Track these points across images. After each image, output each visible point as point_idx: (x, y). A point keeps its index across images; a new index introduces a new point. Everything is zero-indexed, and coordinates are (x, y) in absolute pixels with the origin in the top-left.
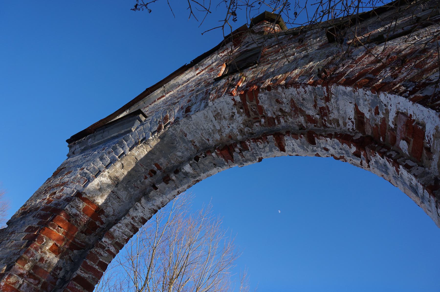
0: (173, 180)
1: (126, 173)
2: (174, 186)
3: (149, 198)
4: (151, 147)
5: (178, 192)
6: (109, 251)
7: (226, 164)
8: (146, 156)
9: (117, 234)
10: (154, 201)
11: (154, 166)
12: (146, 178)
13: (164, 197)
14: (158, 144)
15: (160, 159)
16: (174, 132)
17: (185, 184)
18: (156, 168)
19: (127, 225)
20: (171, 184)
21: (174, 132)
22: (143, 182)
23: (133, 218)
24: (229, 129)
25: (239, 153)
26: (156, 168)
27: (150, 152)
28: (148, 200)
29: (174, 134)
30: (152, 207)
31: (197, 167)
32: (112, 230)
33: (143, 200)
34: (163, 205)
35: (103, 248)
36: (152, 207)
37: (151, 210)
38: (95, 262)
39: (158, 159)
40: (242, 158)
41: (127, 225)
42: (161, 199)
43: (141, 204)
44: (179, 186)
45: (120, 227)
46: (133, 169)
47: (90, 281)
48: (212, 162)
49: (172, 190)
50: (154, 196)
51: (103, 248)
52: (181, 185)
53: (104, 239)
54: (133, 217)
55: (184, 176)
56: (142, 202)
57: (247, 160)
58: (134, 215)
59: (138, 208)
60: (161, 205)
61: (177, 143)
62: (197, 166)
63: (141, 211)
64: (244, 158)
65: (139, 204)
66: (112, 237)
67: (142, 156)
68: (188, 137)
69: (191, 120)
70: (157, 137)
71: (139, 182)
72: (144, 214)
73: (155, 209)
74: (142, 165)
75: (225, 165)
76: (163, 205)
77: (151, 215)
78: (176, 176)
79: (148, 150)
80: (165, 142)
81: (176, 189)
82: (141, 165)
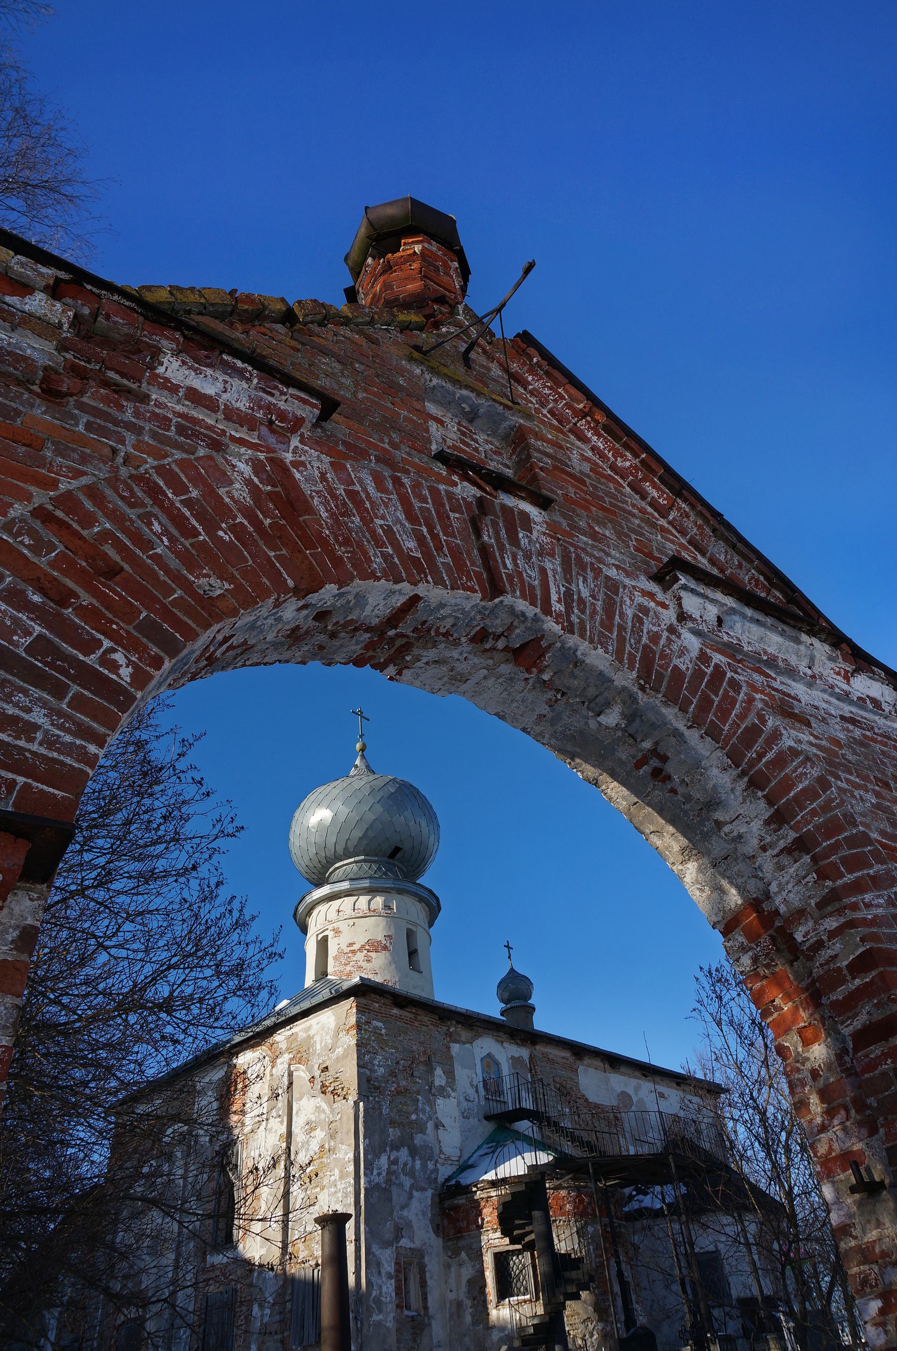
0: (656, 743)
1: (671, 829)
2: (673, 741)
3: (710, 801)
4: (600, 775)
5: (689, 728)
7: (558, 645)
8: (623, 783)
10: (720, 790)
11: (641, 772)
13: (708, 764)
14: (586, 761)
15: (620, 759)
16: (547, 736)
17: (663, 715)
20: (669, 747)
21: (547, 736)
22: (684, 797)
24: (470, 656)
25: (506, 637)
27: (614, 776)
28: (718, 804)
29: (551, 735)
30: (738, 793)
31: (600, 700)
33: (719, 815)
34: (731, 767)
36: (738, 793)
37: (748, 796)
39: (621, 763)
40: (516, 627)
42: (715, 771)
43: (727, 823)
44: (669, 729)
46: (661, 812)
48: (572, 673)
49: (686, 742)
50: (706, 790)
52: (666, 724)
54: (761, 847)
55: (638, 721)
56: (722, 819)
57: (517, 616)
59: (735, 834)
60: (731, 771)
61: (570, 730)
62: (597, 700)
63: (745, 825)
64: (515, 624)
65: (726, 829)
67: (625, 792)
68: (544, 712)
69: (503, 711)
70: (573, 763)
71: (687, 807)
72: (756, 817)
73: (744, 787)
74: (647, 795)
75: (563, 647)
76: (731, 767)
77: (759, 798)
78: (642, 741)
79: (609, 779)
80: (578, 750)
81: (683, 734)
82: (646, 796)
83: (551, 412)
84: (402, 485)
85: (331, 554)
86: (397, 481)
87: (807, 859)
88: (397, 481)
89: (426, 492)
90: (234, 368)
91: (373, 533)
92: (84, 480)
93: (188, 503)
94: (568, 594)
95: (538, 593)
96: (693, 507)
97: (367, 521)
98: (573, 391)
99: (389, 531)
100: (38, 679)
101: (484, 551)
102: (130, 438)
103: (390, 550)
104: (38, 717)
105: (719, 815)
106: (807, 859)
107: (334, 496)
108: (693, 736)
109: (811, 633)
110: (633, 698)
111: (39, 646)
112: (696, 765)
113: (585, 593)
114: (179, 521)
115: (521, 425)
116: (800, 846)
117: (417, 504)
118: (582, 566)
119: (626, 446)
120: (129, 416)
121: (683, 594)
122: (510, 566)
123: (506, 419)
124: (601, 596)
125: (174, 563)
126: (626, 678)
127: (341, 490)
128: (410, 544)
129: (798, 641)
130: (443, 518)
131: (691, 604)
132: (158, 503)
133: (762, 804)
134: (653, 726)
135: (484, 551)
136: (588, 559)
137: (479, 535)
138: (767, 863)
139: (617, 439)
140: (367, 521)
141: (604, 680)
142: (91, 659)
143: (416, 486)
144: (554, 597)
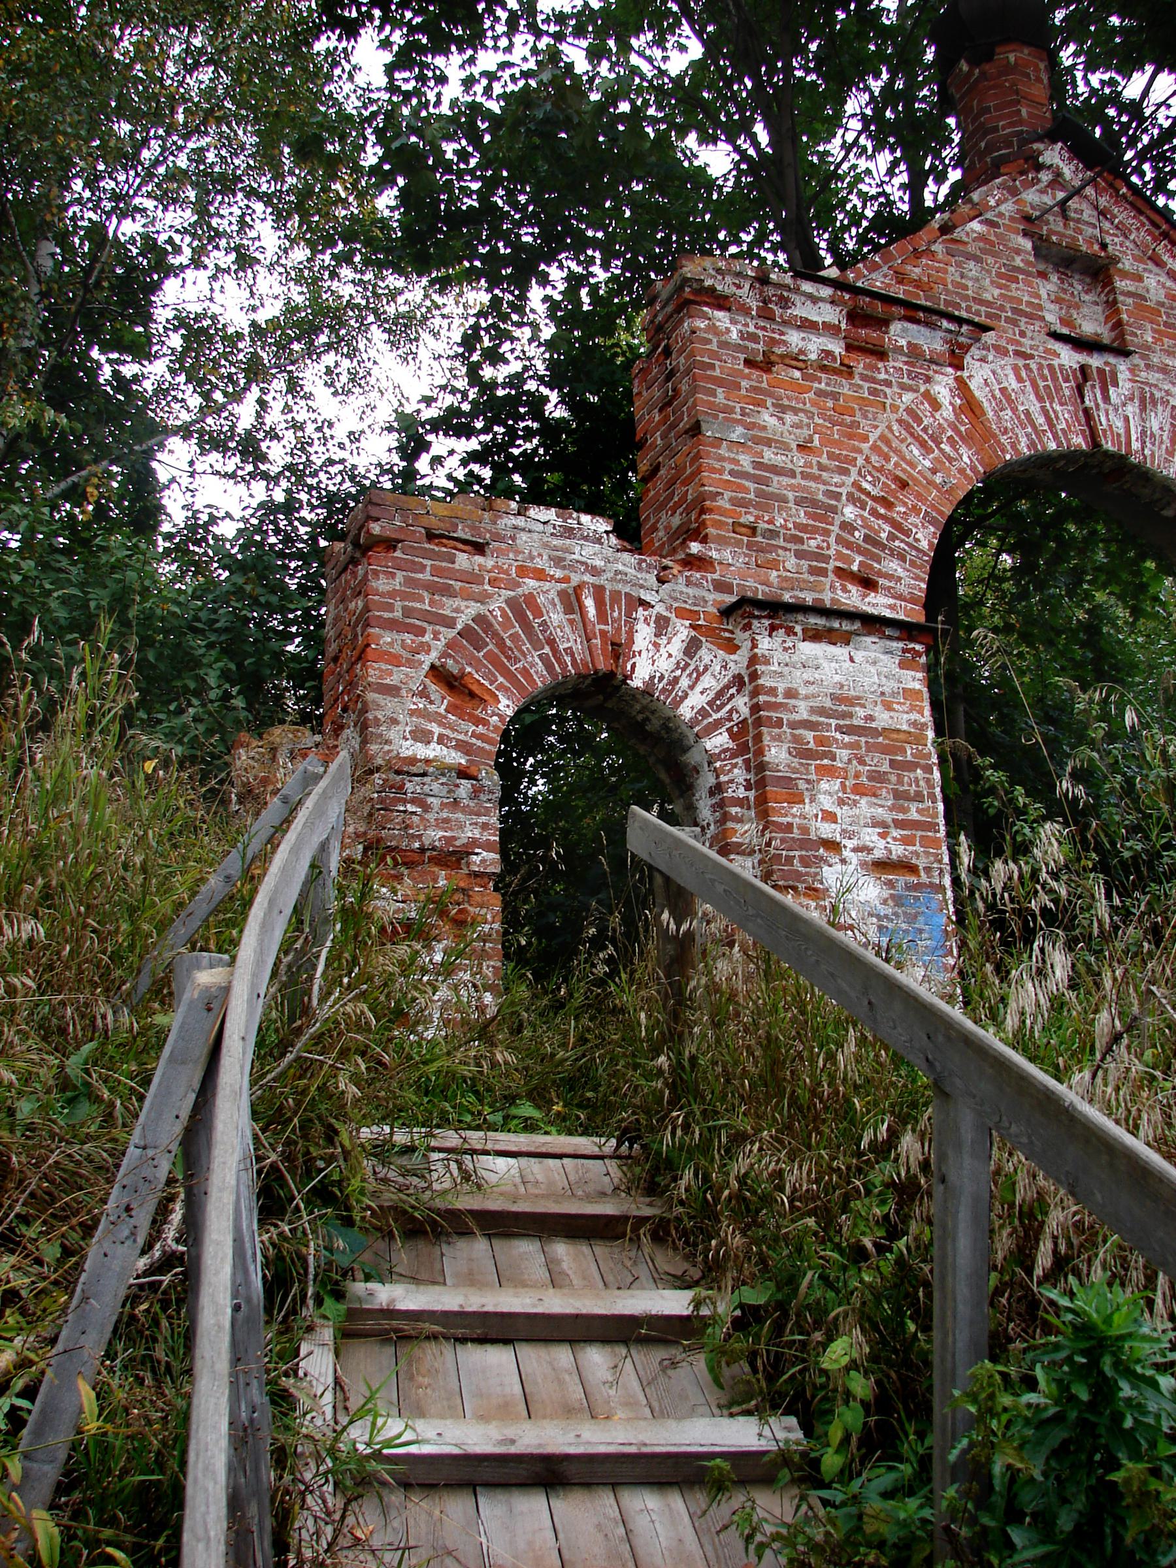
84: (1031, 371)
85: (998, 442)
86: (1027, 367)
88: (1027, 367)
89: (1046, 372)
91: (1018, 418)
92: (878, 432)
93: (925, 430)
94: (1143, 433)
95: (1123, 439)
97: (1014, 410)
99: (1027, 413)
100: (894, 553)
101: (1086, 411)
102: (888, 391)
103: (1029, 430)
104: (900, 572)
107: (994, 396)
111: (892, 537)
113: (1155, 428)
114: (923, 444)
117: (1041, 384)
118: (1154, 402)
120: (883, 376)
122: (1103, 419)
124: (1166, 428)
125: (929, 474)
127: (996, 387)
128: (1041, 420)
130: (1058, 389)
132: (912, 435)
135: (1086, 411)
136: (1158, 395)
137: (1083, 402)
140: (1014, 410)
142: (911, 540)
143: (1040, 367)
144: (1133, 438)
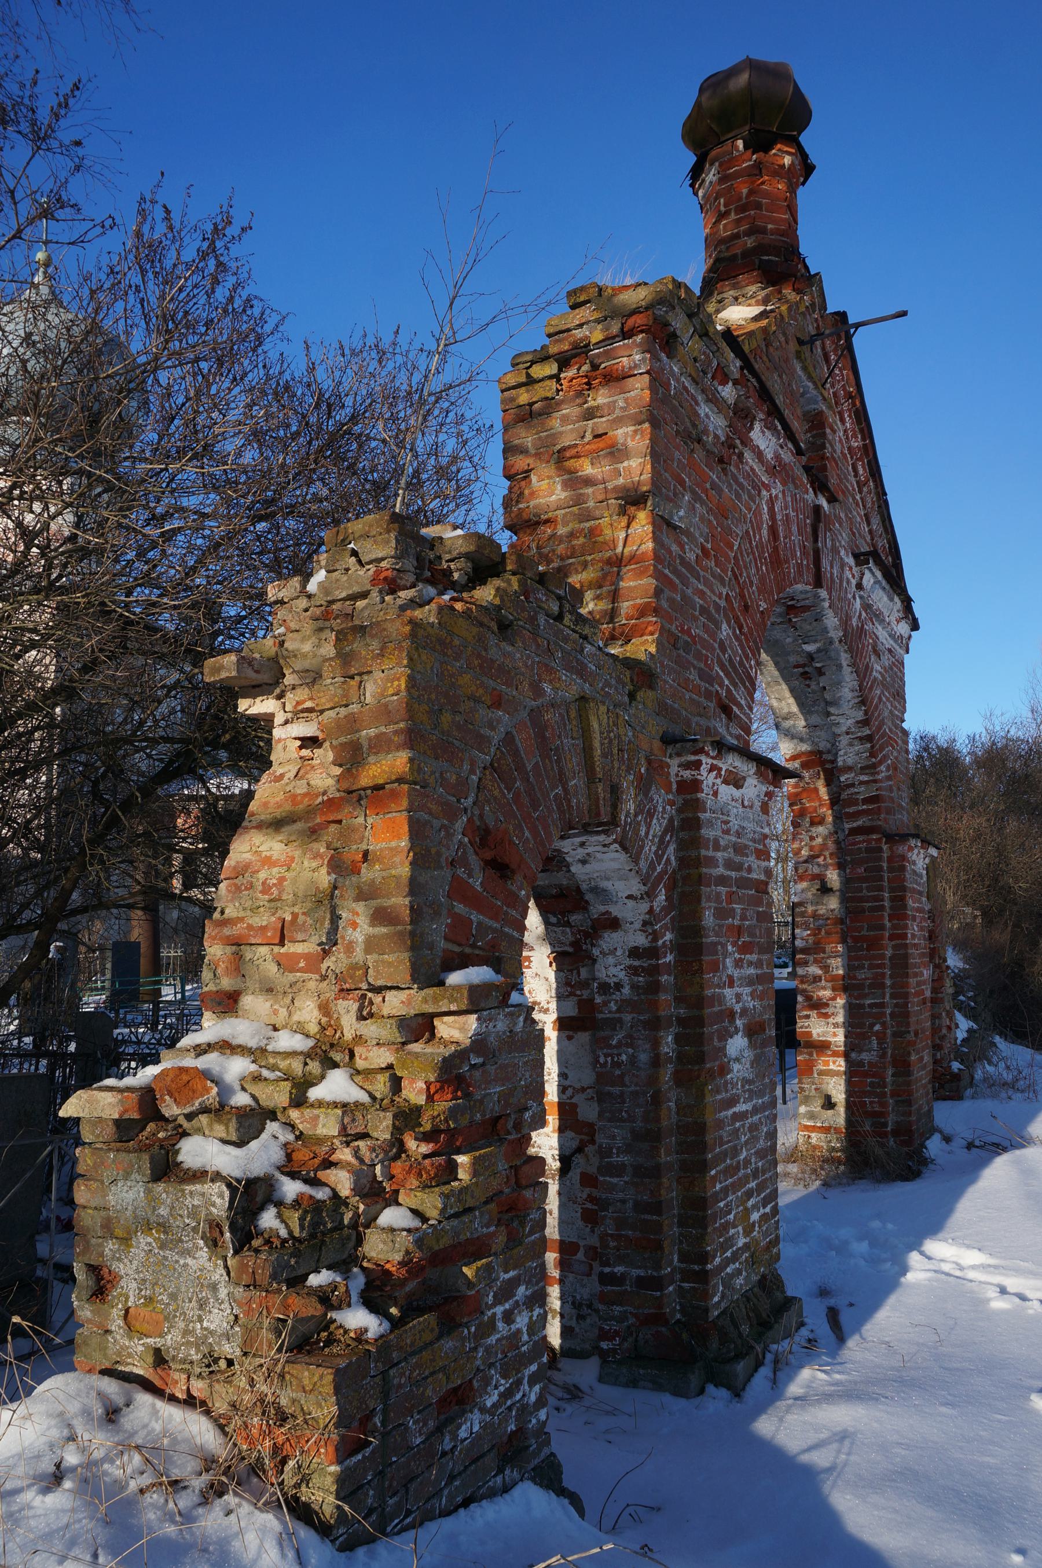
6: (862, 783)
9: (850, 762)
12: (808, 686)
18: (801, 670)
19: (851, 745)
23: (847, 733)
26: (801, 670)
32: (840, 764)
33: (832, 710)
35: (853, 785)
38: (857, 804)
41: (851, 745)
45: (846, 754)
47: (868, 824)
51: (853, 785)
53: (842, 779)
58: (844, 729)
66: (849, 769)
83: (835, 394)
87: (869, 745)
90: (776, 428)
96: (876, 487)
98: (852, 377)
105: (832, 710)
106: (869, 745)
108: (847, 670)
109: (899, 595)
110: (831, 643)
112: (838, 684)
115: (822, 412)
116: (869, 738)
119: (862, 431)
121: (867, 572)
123: (816, 402)
126: (836, 634)
129: (891, 600)
131: (868, 580)
133: (861, 713)
134: (830, 658)
138: (844, 740)
139: (859, 423)
141: (825, 630)
